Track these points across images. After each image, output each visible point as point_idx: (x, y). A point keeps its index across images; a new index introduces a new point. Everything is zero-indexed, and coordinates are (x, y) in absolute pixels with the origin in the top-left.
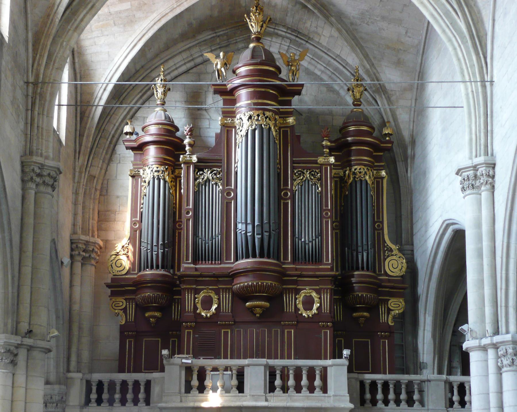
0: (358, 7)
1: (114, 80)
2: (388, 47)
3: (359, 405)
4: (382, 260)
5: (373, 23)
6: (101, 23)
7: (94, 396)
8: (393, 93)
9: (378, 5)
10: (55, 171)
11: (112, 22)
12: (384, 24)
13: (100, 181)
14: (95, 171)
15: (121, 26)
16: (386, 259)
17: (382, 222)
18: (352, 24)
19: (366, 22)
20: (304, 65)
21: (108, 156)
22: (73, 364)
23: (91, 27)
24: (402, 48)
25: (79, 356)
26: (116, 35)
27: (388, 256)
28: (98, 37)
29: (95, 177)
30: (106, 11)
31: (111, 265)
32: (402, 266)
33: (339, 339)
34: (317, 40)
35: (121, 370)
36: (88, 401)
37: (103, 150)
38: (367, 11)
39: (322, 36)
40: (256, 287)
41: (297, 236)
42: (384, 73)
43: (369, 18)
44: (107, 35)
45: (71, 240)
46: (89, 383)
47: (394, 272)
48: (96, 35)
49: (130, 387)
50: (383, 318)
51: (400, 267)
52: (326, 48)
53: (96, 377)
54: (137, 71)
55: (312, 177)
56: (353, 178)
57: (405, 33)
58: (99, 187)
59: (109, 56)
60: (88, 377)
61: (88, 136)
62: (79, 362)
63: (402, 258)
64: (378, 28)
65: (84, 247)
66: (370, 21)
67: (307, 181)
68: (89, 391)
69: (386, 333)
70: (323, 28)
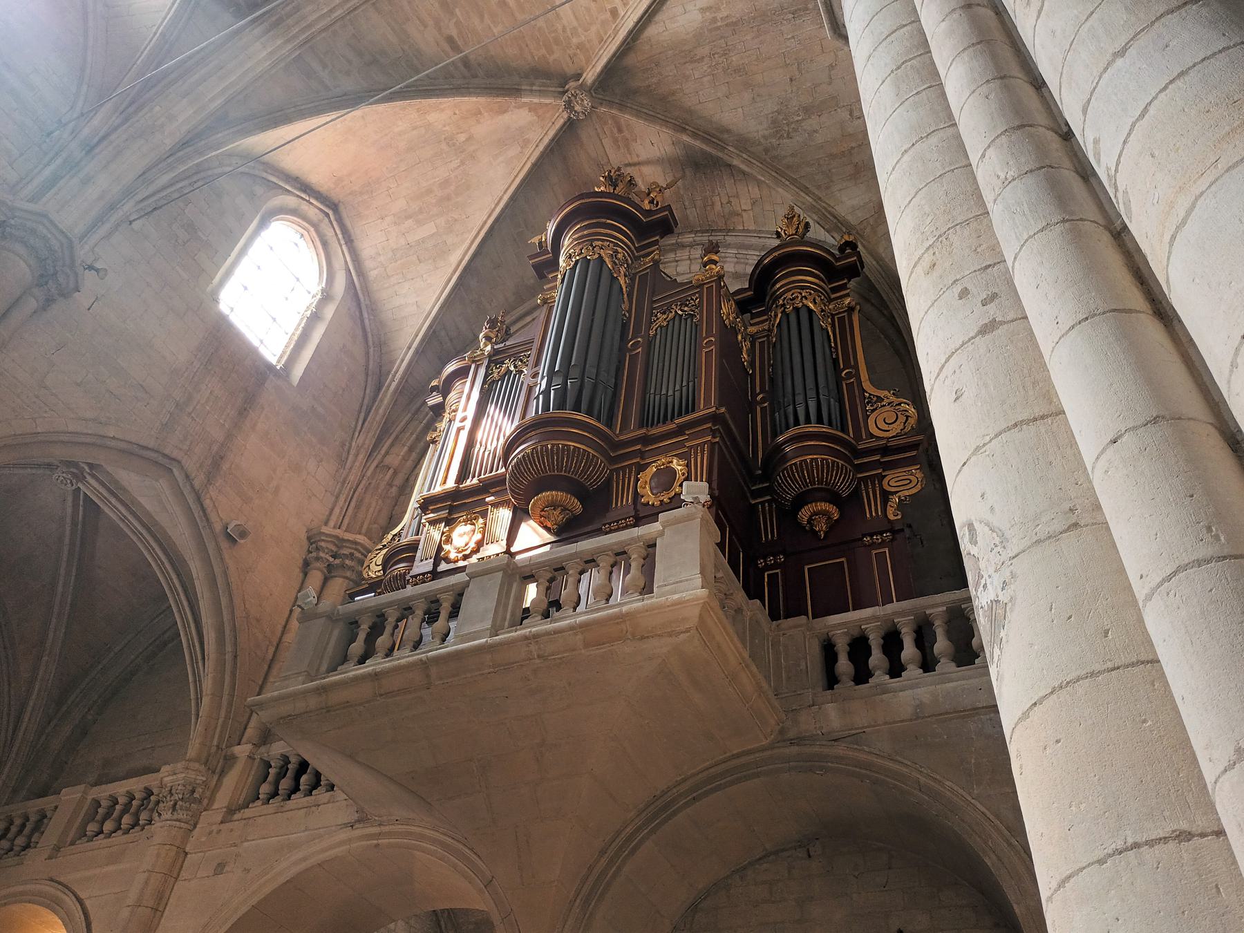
0: (762, 114)
2: (832, 156)
3: (820, 689)
4: (861, 420)
5: (795, 130)
6: (399, 262)
8: (865, 223)
9: (790, 91)
10: (62, 245)
11: (414, 258)
12: (813, 122)
15: (430, 261)
16: (868, 416)
17: (856, 367)
18: (766, 151)
19: (785, 135)
20: (730, 270)
23: (385, 270)
24: (853, 145)
26: (424, 276)
27: (873, 411)
28: (399, 283)
29: (389, 468)
30: (403, 243)
31: (369, 566)
32: (907, 417)
33: (771, 572)
34: (741, 228)
37: (412, 434)
38: (779, 112)
39: (744, 214)
40: (533, 457)
41: (652, 391)
42: (842, 202)
43: (788, 125)
44: (412, 279)
45: (309, 538)
47: (888, 431)
48: (395, 282)
50: (872, 510)
51: (902, 419)
52: (755, 231)
55: (686, 309)
56: (782, 313)
57: (849, 117)
58: (399, 481)
59: (418, 306)
63: (905, 403)
64: (806, 135)
65: (334, 549)
66: (791, 130)
67: (677, 318)
69: (882, 534)
70: (737, 196)
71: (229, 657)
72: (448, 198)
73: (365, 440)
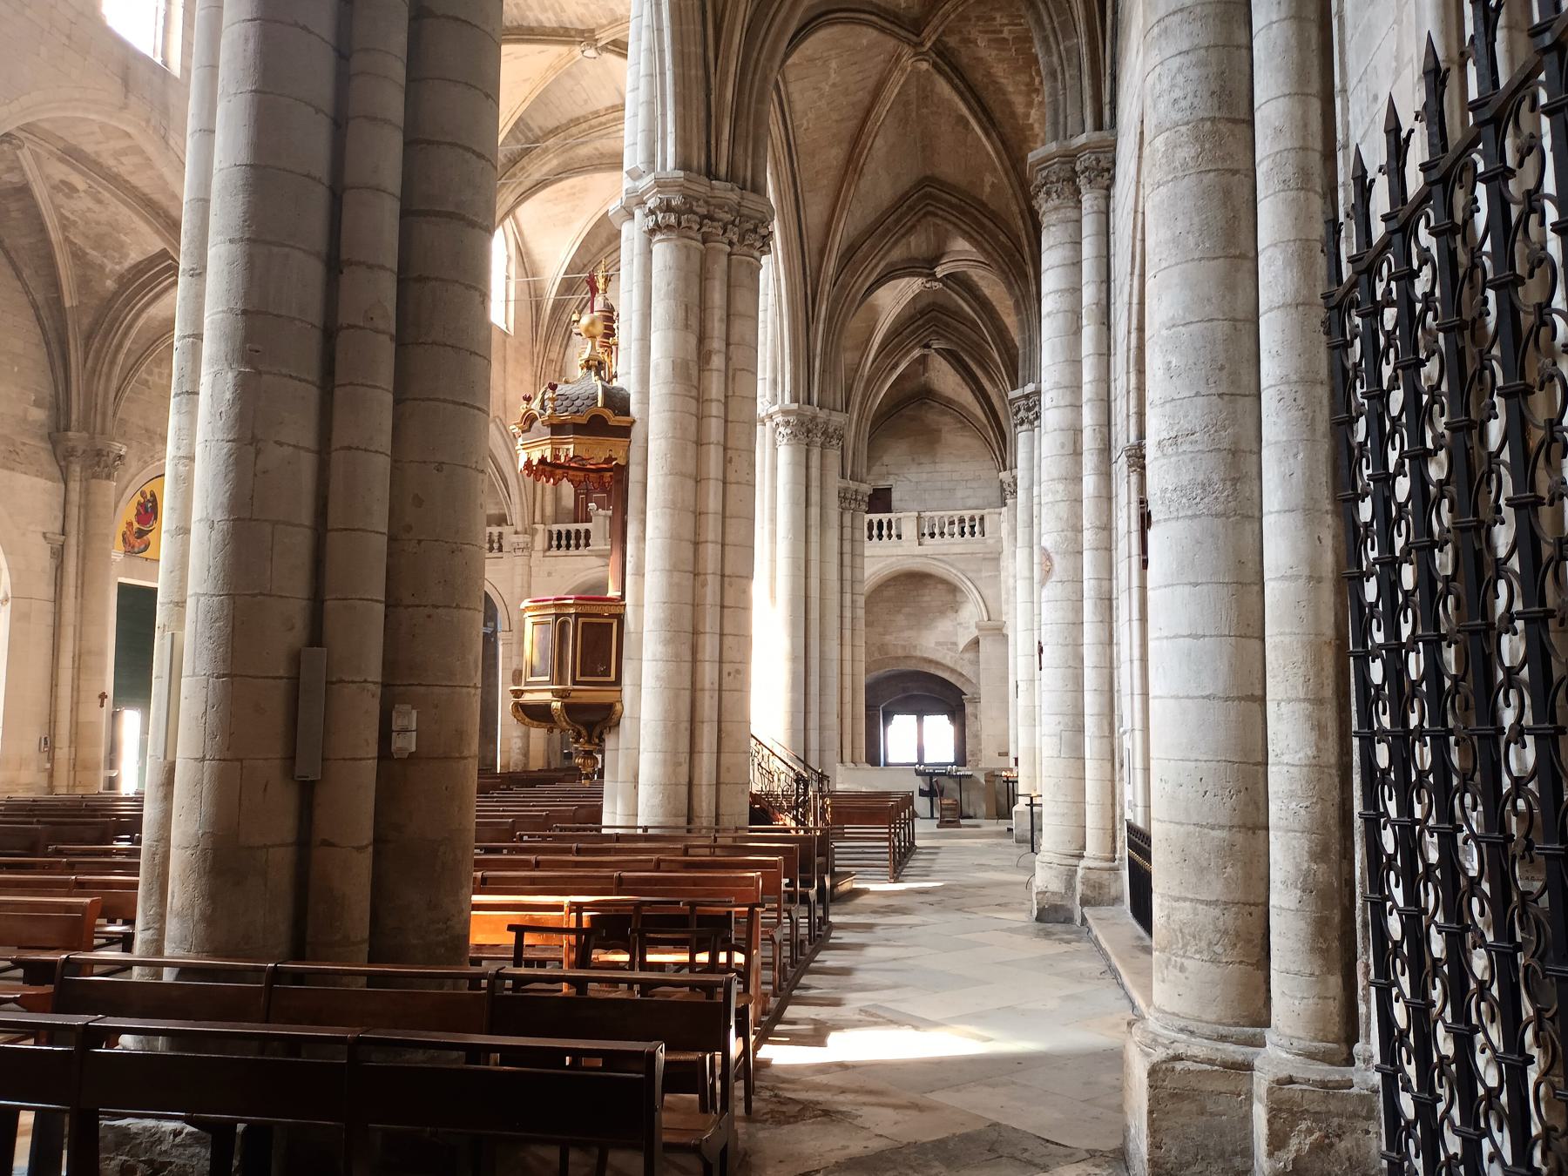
1: (561, 275)
7: (555, 543)
13: (559, 364)
14: (553, 355)
21: (565, 342)
22: (538, 517)
25: (543, 510)
35: (576, 521)
36: (550, 546)
46: (550, 532)
49: (583, 535)
53: (555, 528)
54: (585, 266)
58: (558, 369)
60: (548, 527)
61: (543, 326)
62: (543, 516)
68: (551, 539)
71: (522, 487)
72: (574, 194)
73: (539, 347)
